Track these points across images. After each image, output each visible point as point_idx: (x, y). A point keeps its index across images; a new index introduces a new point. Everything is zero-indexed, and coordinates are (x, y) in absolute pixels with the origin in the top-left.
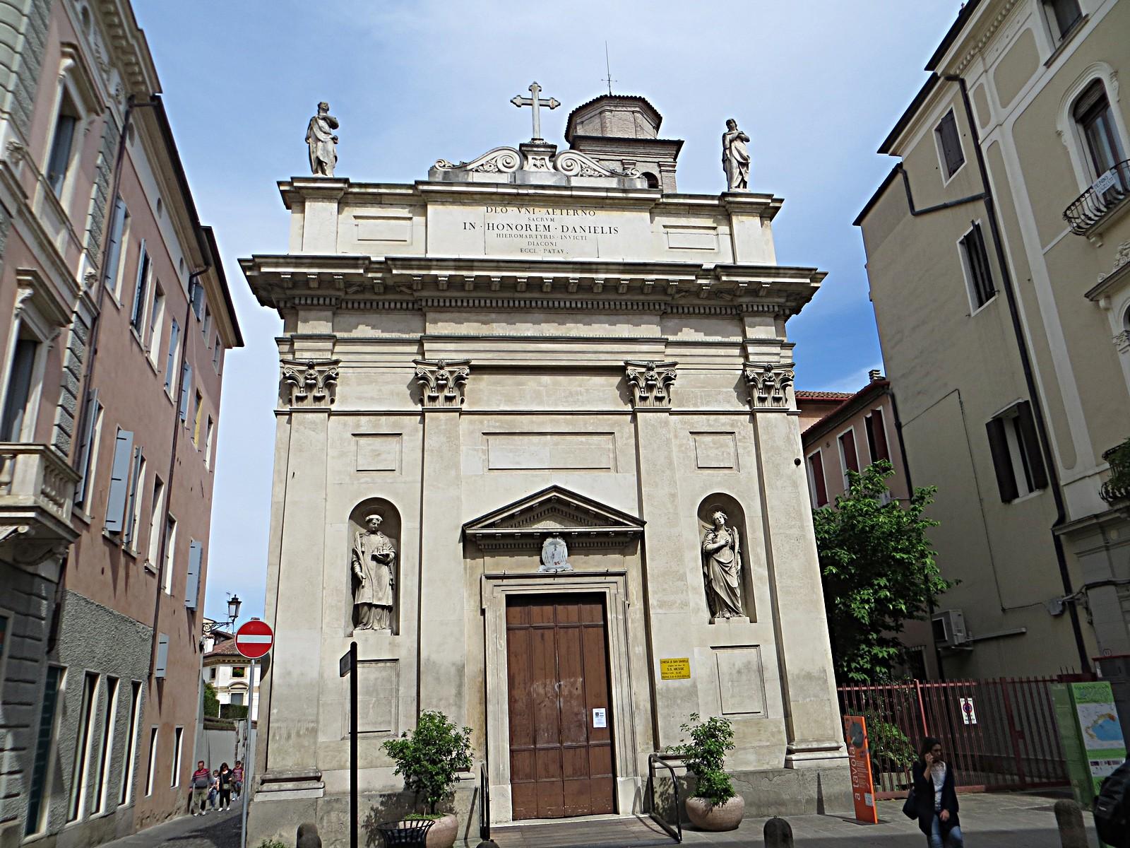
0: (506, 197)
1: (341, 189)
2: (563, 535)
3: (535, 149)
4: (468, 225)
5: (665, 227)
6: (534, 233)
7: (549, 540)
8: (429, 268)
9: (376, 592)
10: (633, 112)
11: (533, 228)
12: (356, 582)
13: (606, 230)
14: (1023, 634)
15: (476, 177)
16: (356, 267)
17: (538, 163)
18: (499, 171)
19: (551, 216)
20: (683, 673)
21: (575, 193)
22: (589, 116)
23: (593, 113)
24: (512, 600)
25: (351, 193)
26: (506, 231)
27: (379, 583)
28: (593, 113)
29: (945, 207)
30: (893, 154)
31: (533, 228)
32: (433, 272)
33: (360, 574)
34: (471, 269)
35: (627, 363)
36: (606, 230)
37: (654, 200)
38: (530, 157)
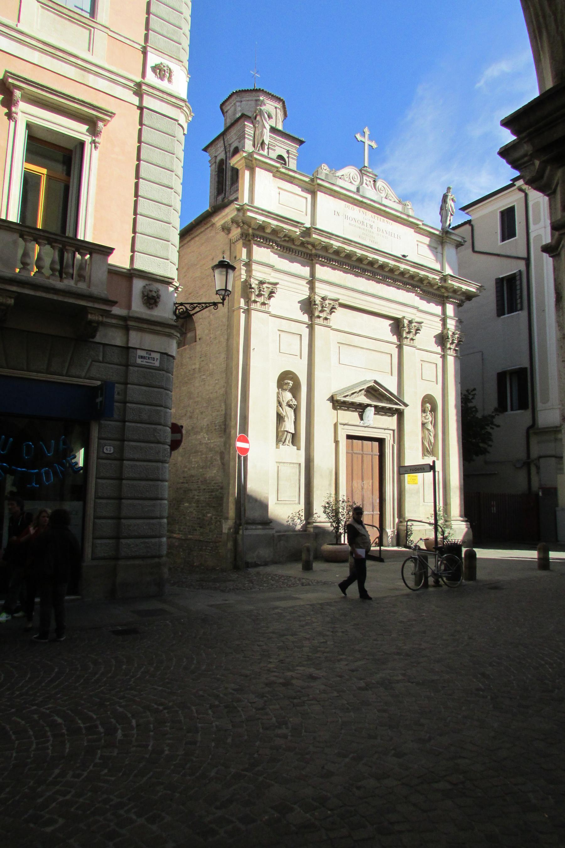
0: (356, 201)
1: (277, 168)
2: (376, 407)
3: (368, 174)
4: (336, 213)
5: (417, 241)
6: (366, 228)
7: (369, 408)
8: (330, 238)
9: (289, 426)
10: (276, 108)
11: (365, 224)
12: (280, 418)
13: (396, 236)
14: (495, 474)
15: (340, 183)
16: (296, 227)
17: (368, 183)
18: (351, 182)
19: (373, 220)
20: (416, 481)
21: (387, 210)
22: (247, 99)
23: (250, 98)
24: (349, 437)
25: (280, 172)
26: (353, 222)
27: (291, 420)
28: (250, 98)
29: (498, 255)
30: (467, 213)
31: (369, 226)
32: (332, 242)
33: (284, 414)
34: (349, 245)
35: (404, 317)
36: (396, 236)
37: (417, 225)
38: (365, 178)
